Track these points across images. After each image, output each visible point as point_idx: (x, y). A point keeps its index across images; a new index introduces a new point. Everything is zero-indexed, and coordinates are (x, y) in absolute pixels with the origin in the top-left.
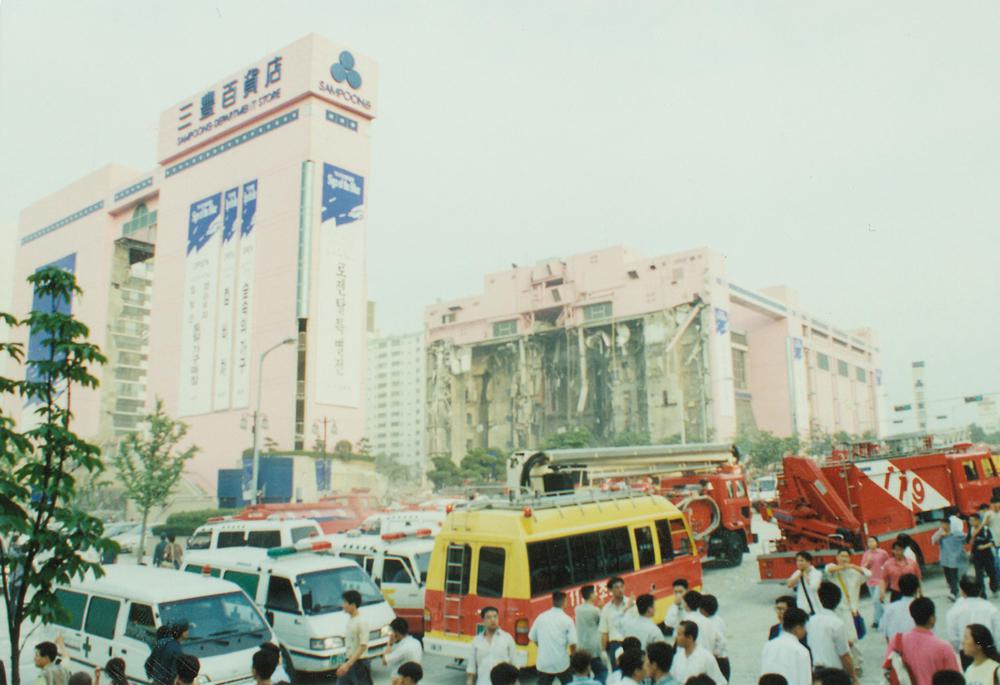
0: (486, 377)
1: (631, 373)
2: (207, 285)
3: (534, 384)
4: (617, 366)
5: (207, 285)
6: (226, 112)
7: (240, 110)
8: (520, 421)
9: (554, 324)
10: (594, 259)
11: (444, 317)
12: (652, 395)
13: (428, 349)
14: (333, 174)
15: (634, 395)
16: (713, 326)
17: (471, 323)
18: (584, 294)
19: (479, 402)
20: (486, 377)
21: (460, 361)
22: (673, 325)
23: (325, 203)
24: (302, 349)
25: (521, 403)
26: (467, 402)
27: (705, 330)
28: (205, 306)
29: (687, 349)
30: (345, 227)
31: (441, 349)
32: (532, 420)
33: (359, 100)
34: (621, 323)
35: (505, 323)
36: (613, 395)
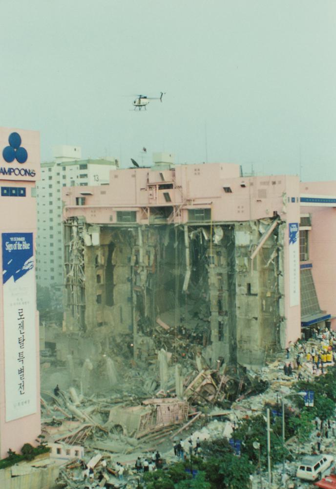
0: (111, 247)
1: (223, 261)
3: (149, 259)
4: (213, 254)
8: (137, 284)
9: (166, 221)
10: (197, 171)
11: (77, 199)
12: (240, 285)
15: (225, 277)
16: (287, 238)
17: (100, 208)
18: (189, 200)
19: (106, 265)
20: (111, 247)
21: (91, 236)
22: (257, 234)
25: (139, 271)
26: (97, 266)
27: (281, 242)
29: (265, 253)
31: (75, 224)
33: (26, 171)
34: (217, 226)
35: (128, 213)
36: (209, 274)
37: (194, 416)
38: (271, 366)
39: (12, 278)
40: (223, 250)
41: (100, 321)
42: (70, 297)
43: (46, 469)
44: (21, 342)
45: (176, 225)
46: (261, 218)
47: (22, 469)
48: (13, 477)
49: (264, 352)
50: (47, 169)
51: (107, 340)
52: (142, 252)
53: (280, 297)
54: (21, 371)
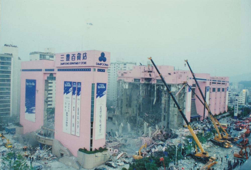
1: (167, 96)
2: (69, 104)
4: (164, 93)
5: (69, 104)
6: (73, 62)
7: (76, 63)
8: (139, 101)
9: (149, 82)
12: (171, 104)
13: (118, 81)
14: (99, 85)
15: (167, 101)
16: (188, 90)
20: (132, 89)
21: (126, 86)
22: (178, 88)
23: (97, 93)
24: (92, 128)
25: (140, 97)
27: (186, 91)
28: (69, 108)
29: (180, 94)
30: (101, 98)
31: (121, 81)
32: (142, 102)
33: (105, 64)
35: (137, 79)
36: (162, 100)
37: (154, 143)
38: (180, 130)
39: (99, 97)
40: (167, 93)
41: (127, 112)
42: (118, 104)
43: (106, 155)
44: (101, 116)
45: (152, 84)
46: (180, 83)
47: (99, 154)
48: (96, 156)
49: (178, 125)
50: (114, 64)
51: (129, 118)
52: (141, 91)
53: (184, 109)
54: (100, 125)
